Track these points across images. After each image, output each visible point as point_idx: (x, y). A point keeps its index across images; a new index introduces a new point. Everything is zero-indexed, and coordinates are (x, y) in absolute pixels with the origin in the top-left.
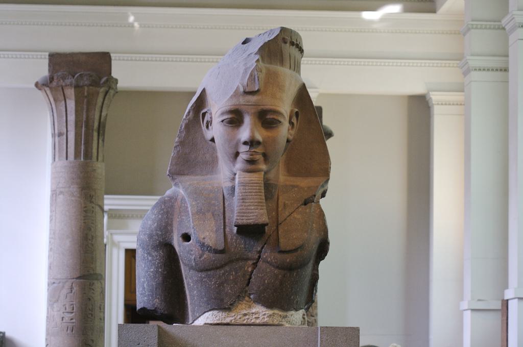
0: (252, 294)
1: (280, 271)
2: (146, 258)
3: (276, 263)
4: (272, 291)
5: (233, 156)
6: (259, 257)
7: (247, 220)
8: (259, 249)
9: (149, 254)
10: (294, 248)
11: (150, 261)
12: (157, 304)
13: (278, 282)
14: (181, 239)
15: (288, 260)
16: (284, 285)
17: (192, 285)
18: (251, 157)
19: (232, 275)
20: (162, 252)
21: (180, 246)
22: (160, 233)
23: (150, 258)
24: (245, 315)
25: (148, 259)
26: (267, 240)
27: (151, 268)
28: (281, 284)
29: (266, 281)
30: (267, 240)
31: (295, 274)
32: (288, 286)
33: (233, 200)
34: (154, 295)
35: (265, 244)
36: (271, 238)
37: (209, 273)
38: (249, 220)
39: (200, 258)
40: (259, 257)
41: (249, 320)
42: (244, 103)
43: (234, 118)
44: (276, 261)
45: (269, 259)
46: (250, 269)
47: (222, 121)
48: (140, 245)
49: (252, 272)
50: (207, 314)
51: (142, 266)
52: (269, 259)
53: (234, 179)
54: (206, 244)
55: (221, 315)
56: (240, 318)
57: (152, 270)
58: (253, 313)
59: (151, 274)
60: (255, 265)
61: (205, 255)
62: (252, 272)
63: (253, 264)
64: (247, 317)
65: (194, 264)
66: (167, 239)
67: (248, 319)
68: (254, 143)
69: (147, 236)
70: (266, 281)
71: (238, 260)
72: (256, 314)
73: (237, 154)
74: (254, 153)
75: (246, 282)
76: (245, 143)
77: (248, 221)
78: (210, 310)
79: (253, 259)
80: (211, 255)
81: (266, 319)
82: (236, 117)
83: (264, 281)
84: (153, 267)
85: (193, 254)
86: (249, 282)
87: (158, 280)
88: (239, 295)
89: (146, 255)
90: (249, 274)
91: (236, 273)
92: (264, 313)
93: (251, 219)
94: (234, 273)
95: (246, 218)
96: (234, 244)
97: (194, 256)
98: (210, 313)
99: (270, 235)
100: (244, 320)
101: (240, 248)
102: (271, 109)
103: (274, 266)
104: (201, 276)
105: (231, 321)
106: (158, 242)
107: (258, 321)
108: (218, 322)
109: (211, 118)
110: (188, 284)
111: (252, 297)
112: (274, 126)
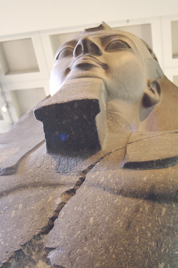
0: (52, 249)
1: (126, 199)
3: (116, 184)
4: (106, 240)
8: (85, 168)
10: (157, 158)
13: (120, 222)
15: (145, 179)
16: (137, 229)
18: (84, 60)
26: (102, 158)
28: (129, 226)
29: (91, 220)
30: (102, 158)
31: (164, 210)
32: (149, 234)
35: (98, 161)
36: (111, 155)
40: (83, 180)
43: (70, 48)
44: (118, 179)
45: (102, 180)
46: (59, 201)
47: (57, 59)
49: (62, 205)
62: (62, 205)
68: (89, 45)
70: (91, 220)
74: (88, 57)
75: (45, 224)
83: (88, 218)
86: (50, 227)
88: (20, 251)
96: (38, 164)
99: (112, 152)
102: (116, 34)
103: (112, 191)
111: (52, 255)
112: (122, 49)
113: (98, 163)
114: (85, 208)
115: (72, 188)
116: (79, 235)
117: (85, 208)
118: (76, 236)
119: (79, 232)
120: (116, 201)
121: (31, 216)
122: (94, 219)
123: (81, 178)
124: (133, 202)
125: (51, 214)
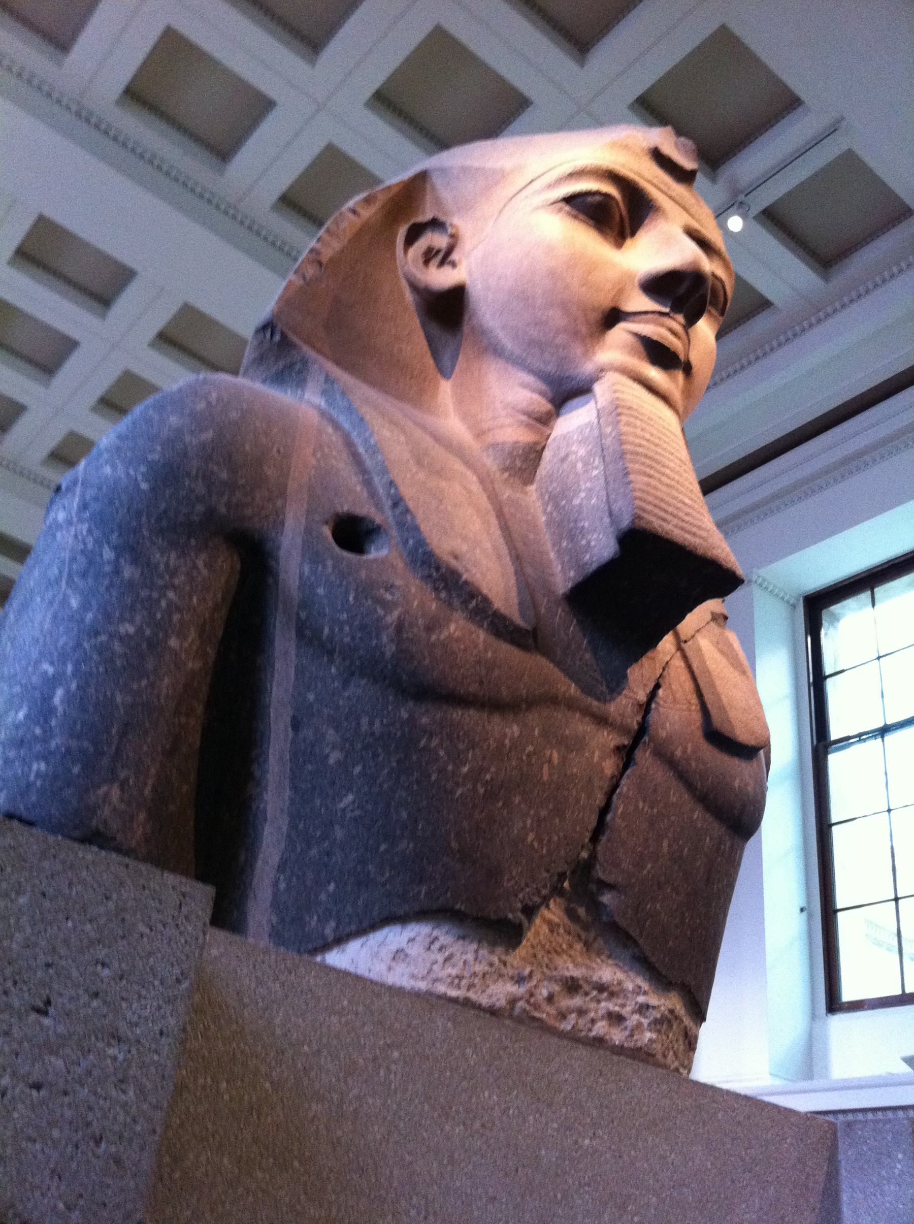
0: (611, 887)
2: (108, 569)
5: (594, 316)
6: (643, 728)
7: (676, 526)
8: (642, 696)
9: (131, 549)
11: (131, 585)
12: (107, 811)
14: (327, 531)
17: (335, 757)
19: (550, 761)
20: (205, 566)
21: (314, 556)
22: (224, 475)
23: (128, 572)
24: (572, 986)
25: (117, 571)
27: (122, 619)
29: (665, 844)
30: (661, 675)
33: (526, 493)
34: (105, 761)
37: (457, 714)
38: (689, 532)
39: (429, 629)
40: (643, 728)
41: (581, 1022)
42: (650, 178)
43: (617, 203)
47: (569, 200)
48: (84, 506)
50: (394, 937)
51: (65, 602)
52: (678, 753)
53: (545, 420)
54: (464, 577)
55: (470, 957)
56: (550, 999)
57: (128, 628)
58: (601, 988)
59: (117, 647)
60: (626, 755)
61: (452, 627)
63: (618, 749)
64: (577, 1001)
65: (390, 649)
66: (248, 512)
67: (581, 1012)
69: (143, 469)
70: (665, 844)
71: (571, 705)
72: (612, 995)
73: (613, 316)
76: (661, 285)
77: (687, 536)
78: (421, 915)
79: (622, 729)
80: (482, 636)
81: (648, 1035)
82: (621, 204)
84: (138, 618)
85: (395, 604)
87: (152, 685)
89: (108, 554)
90: (606, 785)
91: (564, 760)
92: (641, 999)
93: (694, 534)
94: (555, 755)
95: (675, 521)
97: (396, 613)
98: (420, 931)
100: (563, 1016)
101: (581, 660)
103: (690, 786)
104: (412, 721)
105: (513, 1001)
106: (200, 508)
107: (617, 1036)
108: (453, 993)
109: (455, 239)
110: (303, 756)
113: (661, 692)
114: (655, 810)
115: (626, 743)
116: (649, 872)
117: (655, 810)
118: (645, 872)
119: (649, 866)
120: (695, 817)
121: (574, 793)
122: (670, 845)
123: (638, 723)
124: (717, 829)
125: (599, 799)
